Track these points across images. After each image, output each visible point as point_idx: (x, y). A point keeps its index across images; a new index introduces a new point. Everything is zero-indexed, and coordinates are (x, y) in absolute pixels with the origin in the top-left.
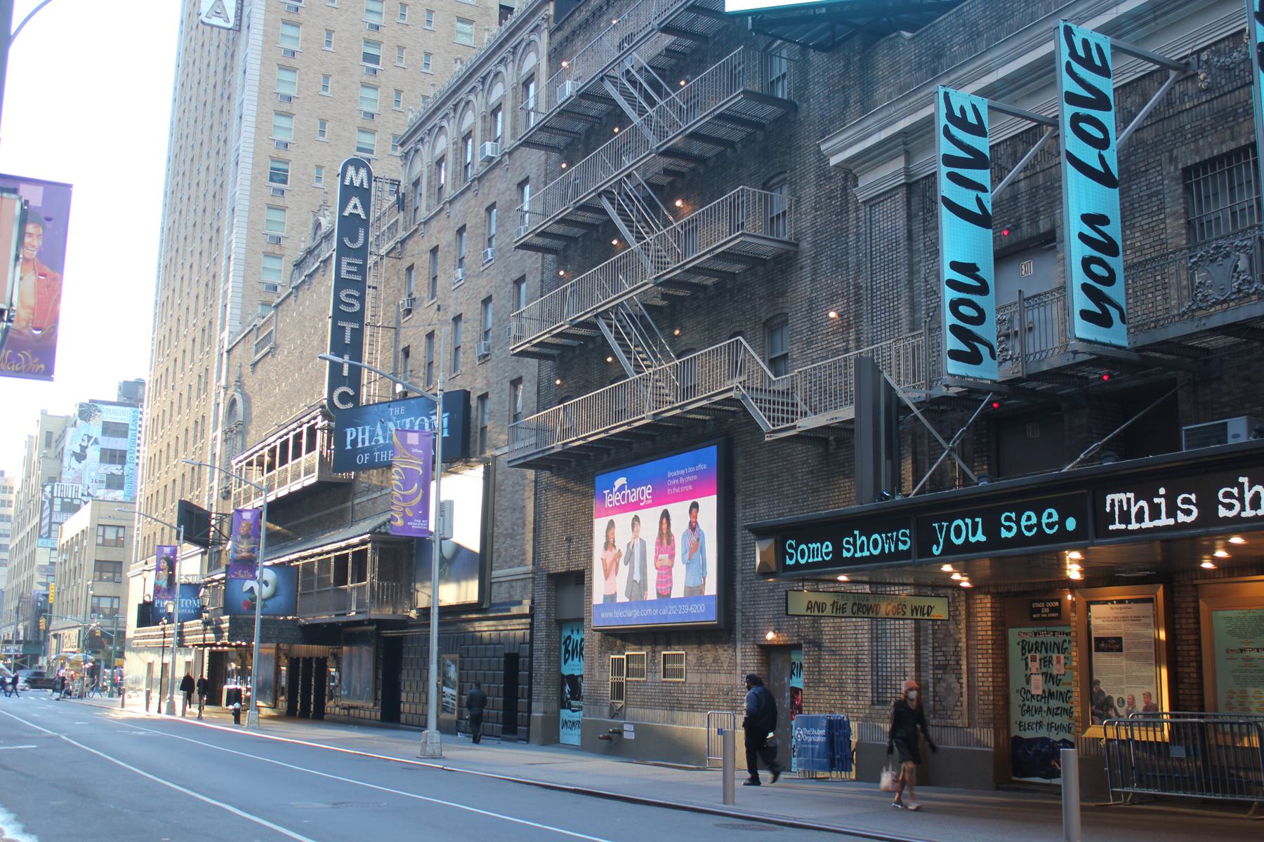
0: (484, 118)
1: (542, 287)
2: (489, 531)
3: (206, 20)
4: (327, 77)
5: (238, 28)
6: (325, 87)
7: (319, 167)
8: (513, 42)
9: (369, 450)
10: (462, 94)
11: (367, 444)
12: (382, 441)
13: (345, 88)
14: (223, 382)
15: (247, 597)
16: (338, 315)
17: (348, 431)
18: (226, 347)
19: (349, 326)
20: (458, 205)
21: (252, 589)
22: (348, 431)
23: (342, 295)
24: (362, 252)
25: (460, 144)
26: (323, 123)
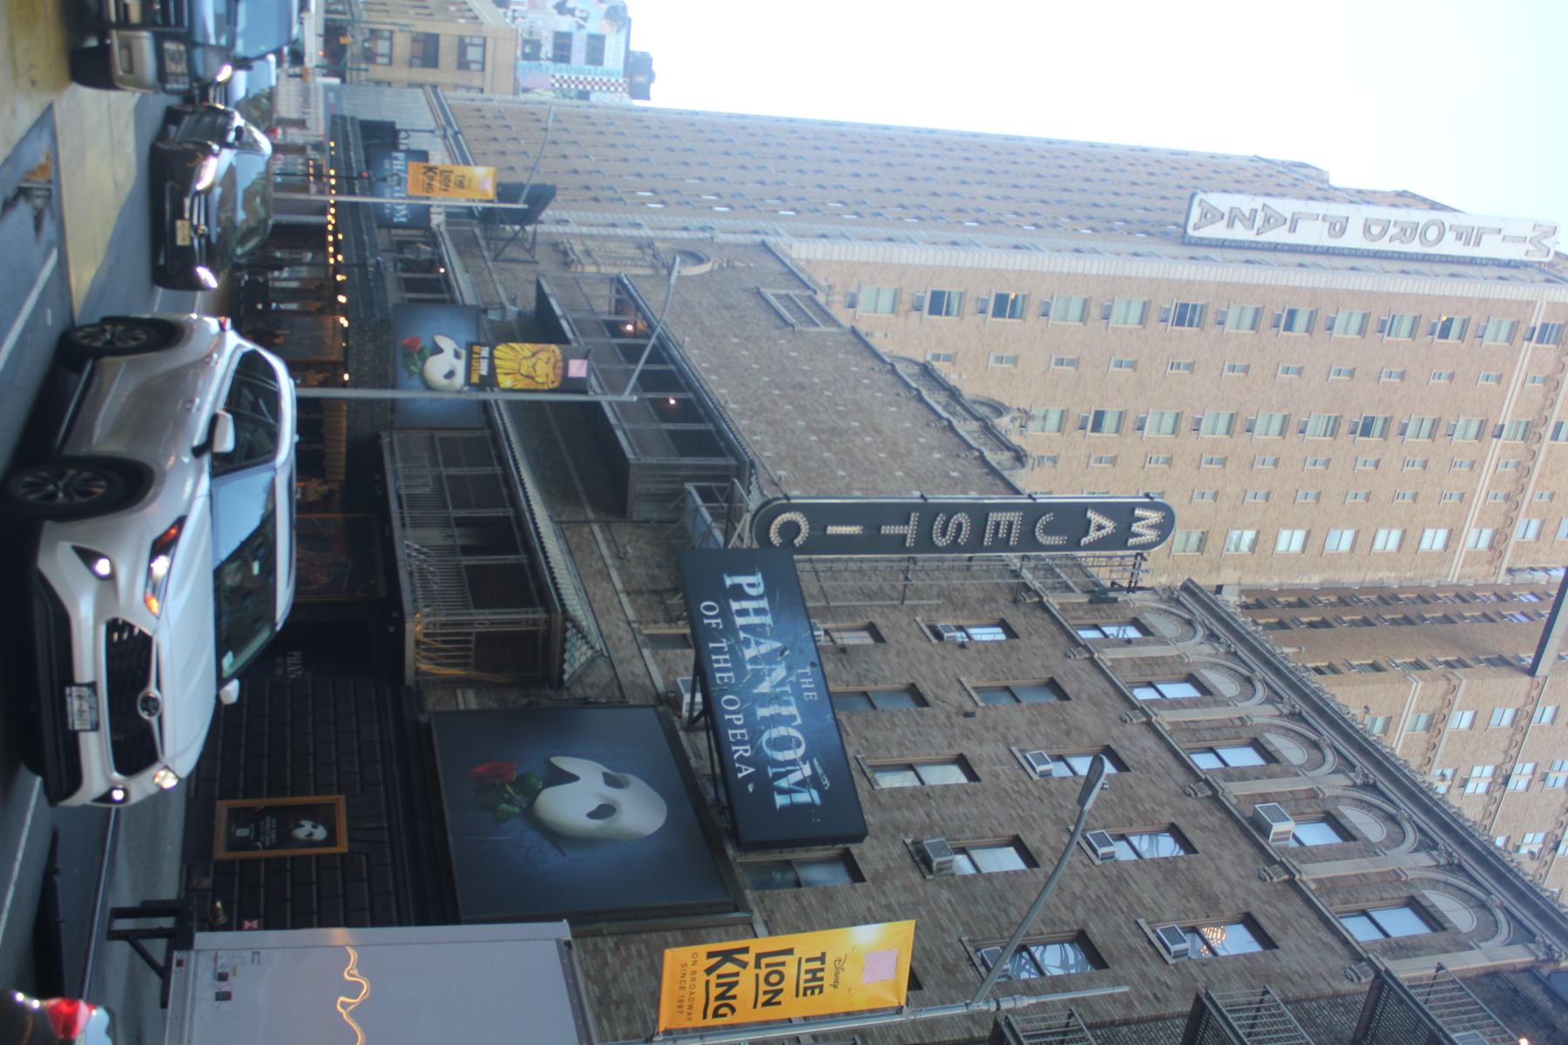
0: (1313, 795)
1: (1102, 1025)
2: (604, 927)
3: (1196, 200)
4: (1133, 365)
5: (1185, 241)
6: (1120, 364)
7: (1015, 360)
8: (1470, 864)
9: (730, 629)
10: (1329, 735)
11: (740, 621)
12: (749, 653)
14: (721, 237)
15: (425, 343)
16: (928, 512)
17: (757, 579)
18: (771, 240)
19: (909, 531)
20: (1150, 742)
21: (438, 350)
22: (757, 579)
23: (961, 517)
24: (1028, 542)
25: (1246, 735)
26: (1074, 363)
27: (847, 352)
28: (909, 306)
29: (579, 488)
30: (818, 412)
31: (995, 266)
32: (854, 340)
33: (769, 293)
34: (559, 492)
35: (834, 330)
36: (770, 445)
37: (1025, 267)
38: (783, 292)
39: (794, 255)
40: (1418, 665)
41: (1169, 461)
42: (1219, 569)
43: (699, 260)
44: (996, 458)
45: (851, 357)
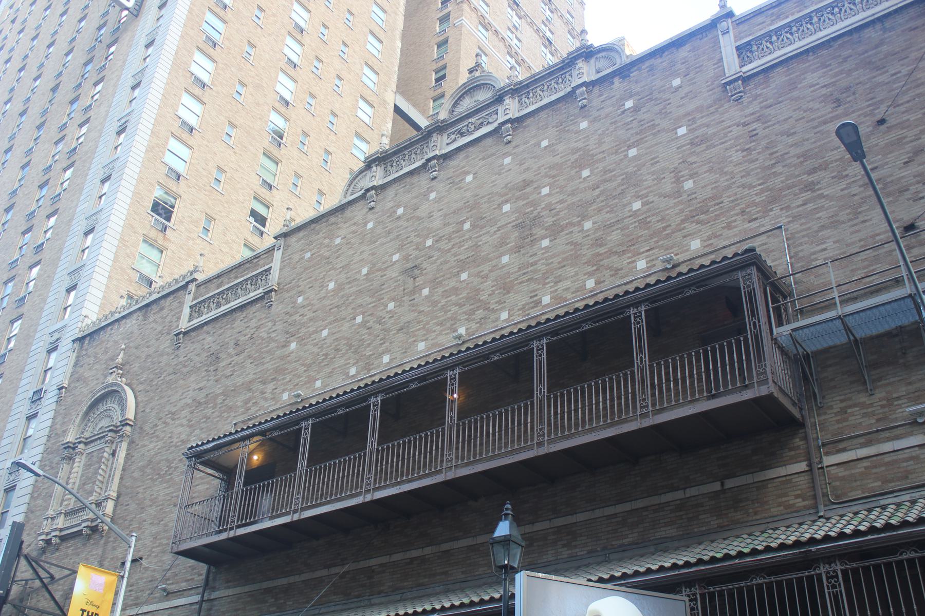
13: (258, 104)
27: (332, 237)
28: (160, 234)
29: (717, 486)
30: (476, 246)
31: (144, 149)
32: (301, 234)
33: (184, 325)
34: (732, 511)
35: (278, 255)
36: (566, 284)
37: (151, 126)
38: (186, 311)
39: (94, 317)
40: (445, 19)
41: (313, 96)
42: (385, 101)
43: (112, 394)
44: (586, 72)
45: (342, 232)
